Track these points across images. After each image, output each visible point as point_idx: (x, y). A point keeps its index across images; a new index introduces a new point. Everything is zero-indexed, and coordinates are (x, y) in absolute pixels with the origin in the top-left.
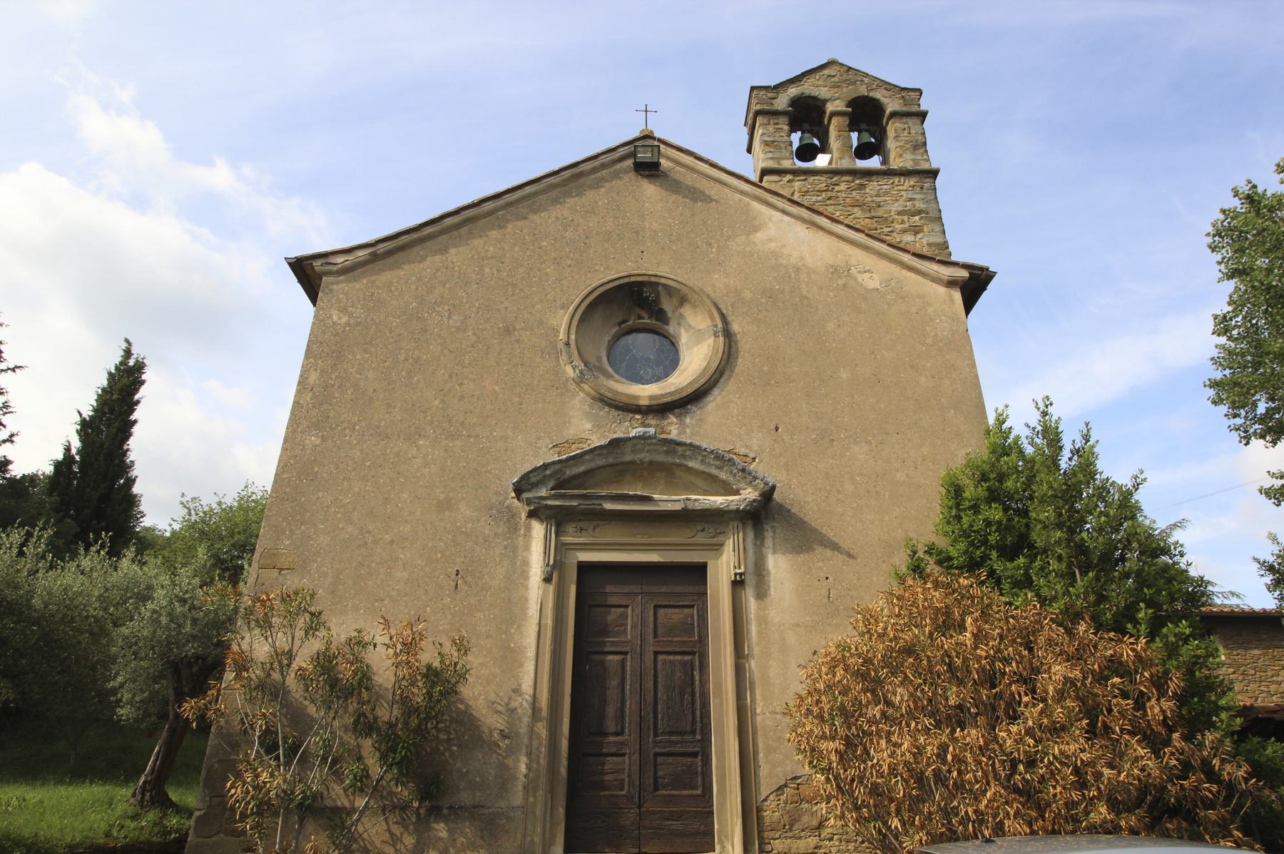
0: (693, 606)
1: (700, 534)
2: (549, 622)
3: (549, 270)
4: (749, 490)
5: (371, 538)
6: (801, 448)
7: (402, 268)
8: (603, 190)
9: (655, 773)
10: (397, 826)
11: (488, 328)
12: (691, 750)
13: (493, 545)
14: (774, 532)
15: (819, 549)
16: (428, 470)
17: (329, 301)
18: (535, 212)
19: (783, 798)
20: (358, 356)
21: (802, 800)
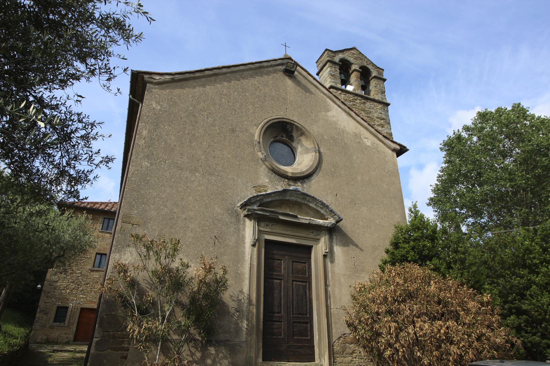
2: (255, 263)
4: (332, 219)
9: (293, 329)
14: (336, 237)
15: (351, 246)
17: (151, 96)
18: (243, 78)
19: (340, 341)
20: (166, 127)
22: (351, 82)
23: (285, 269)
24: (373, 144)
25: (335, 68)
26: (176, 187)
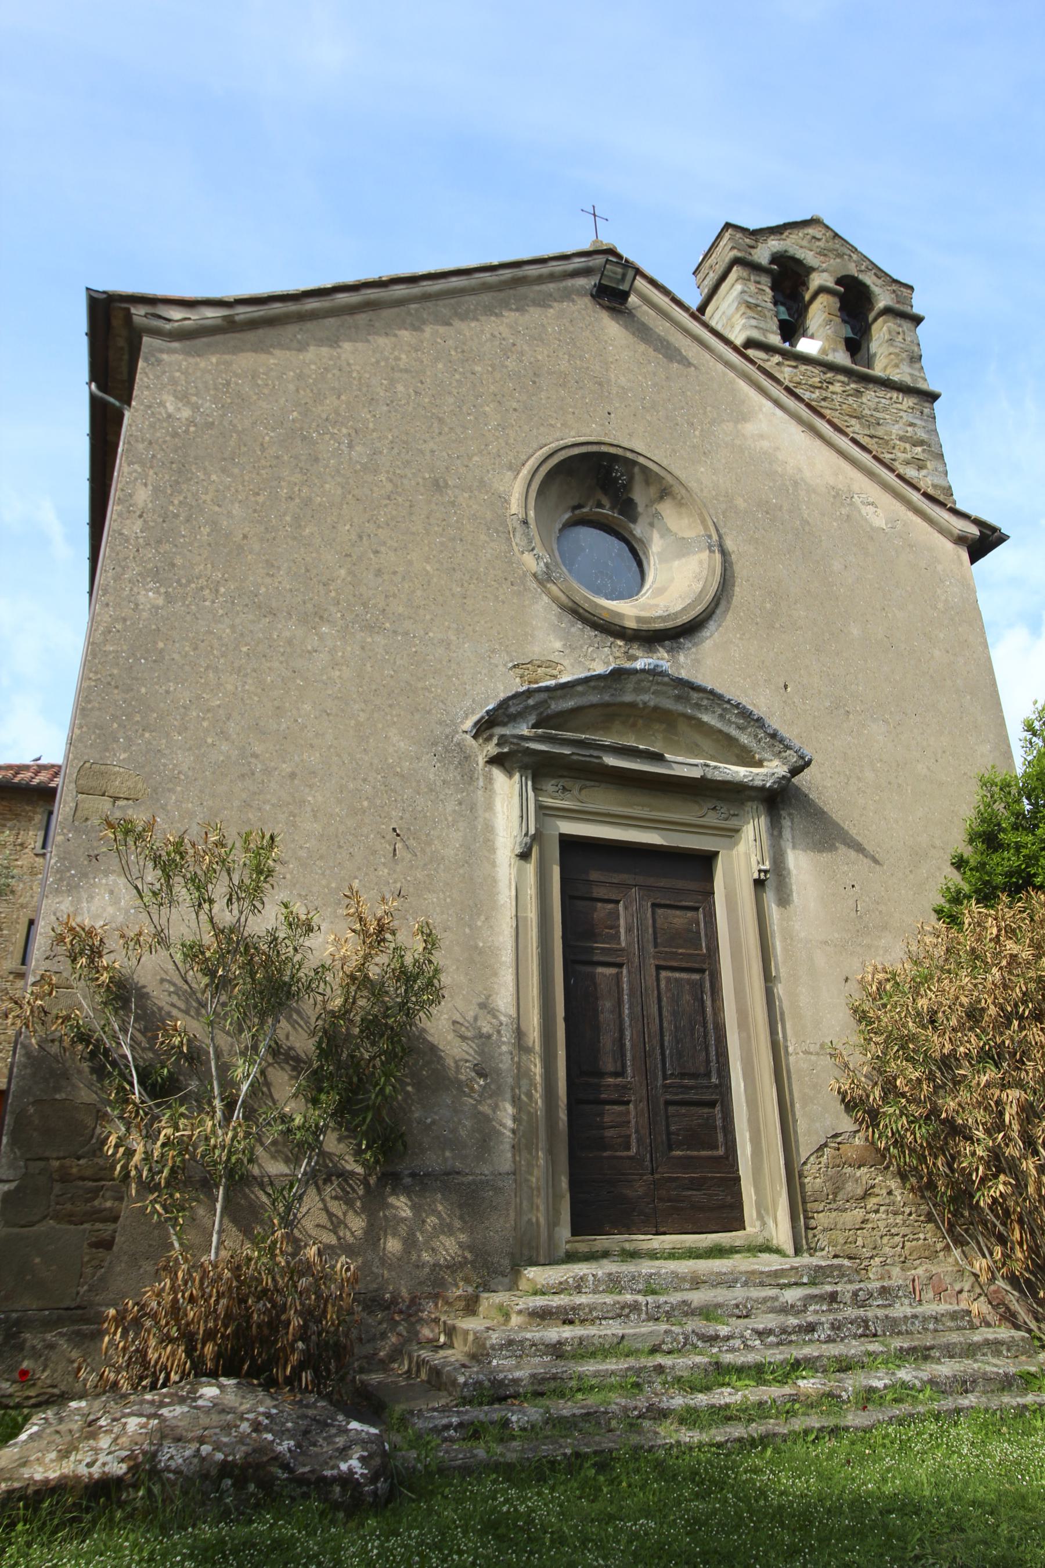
0: (696, 909)
1: (711, 813)
2: (532, 914)
3: (487, 409)
4: (776, 762)
5: (259, 766)
6: (815, 717)
7: (271, 353)
8: (551, 310)
9: (668, 1126)
10: (336, 1203)
11: (410, 475)
12: (707, 1097)
13: (442, 797)
14: (792, 821)
15: (842, 849)
16: (338, 673)
18: (463, 317)
19: (824, 1160)
20: (214, 477)
21: (844, 1164)
22: (810, 331)
23: (629, 930)
24: (893, 521)
25: (759, 283)
26: (254, 670)
